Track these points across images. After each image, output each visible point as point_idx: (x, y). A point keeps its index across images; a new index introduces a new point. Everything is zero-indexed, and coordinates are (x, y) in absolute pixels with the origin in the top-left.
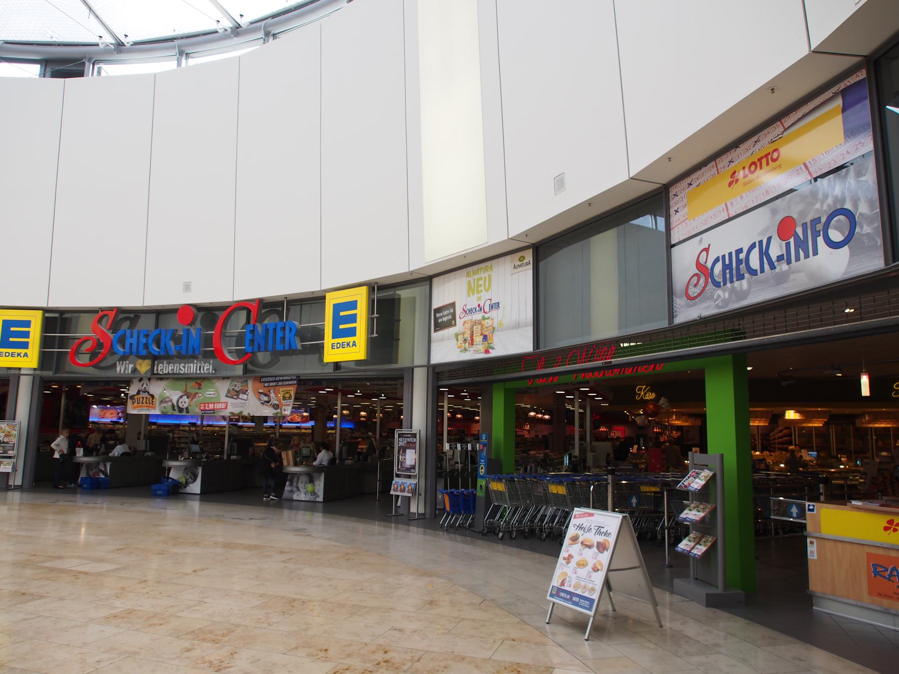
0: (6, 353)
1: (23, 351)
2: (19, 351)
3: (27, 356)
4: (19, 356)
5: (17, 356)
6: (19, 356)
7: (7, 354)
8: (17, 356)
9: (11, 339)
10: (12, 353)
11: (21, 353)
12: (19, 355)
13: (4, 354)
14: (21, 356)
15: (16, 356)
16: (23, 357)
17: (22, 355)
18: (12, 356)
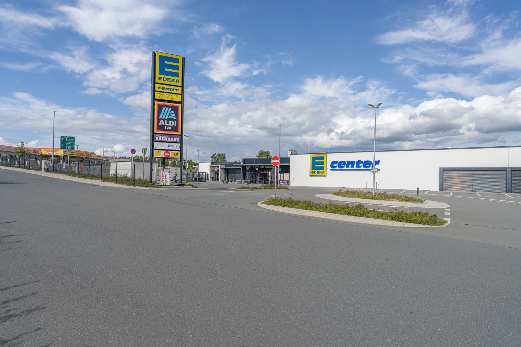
0: (164, 78)
1: (176, 78)
2: (173, 78)
3: (179, 83)
4: (173, 82)
5: (172, 82)
6: (173, 82)
7: (165, 79)
8: (172, 82)
9: (166, 70)
10: (168, 78)
11: (174, 79)
12: (173, 80)
13: (163, 78)
14: (174, 82)
15: (171, 81)
16: (176, 82)
17: (175, 81)
18: (168, 81)
